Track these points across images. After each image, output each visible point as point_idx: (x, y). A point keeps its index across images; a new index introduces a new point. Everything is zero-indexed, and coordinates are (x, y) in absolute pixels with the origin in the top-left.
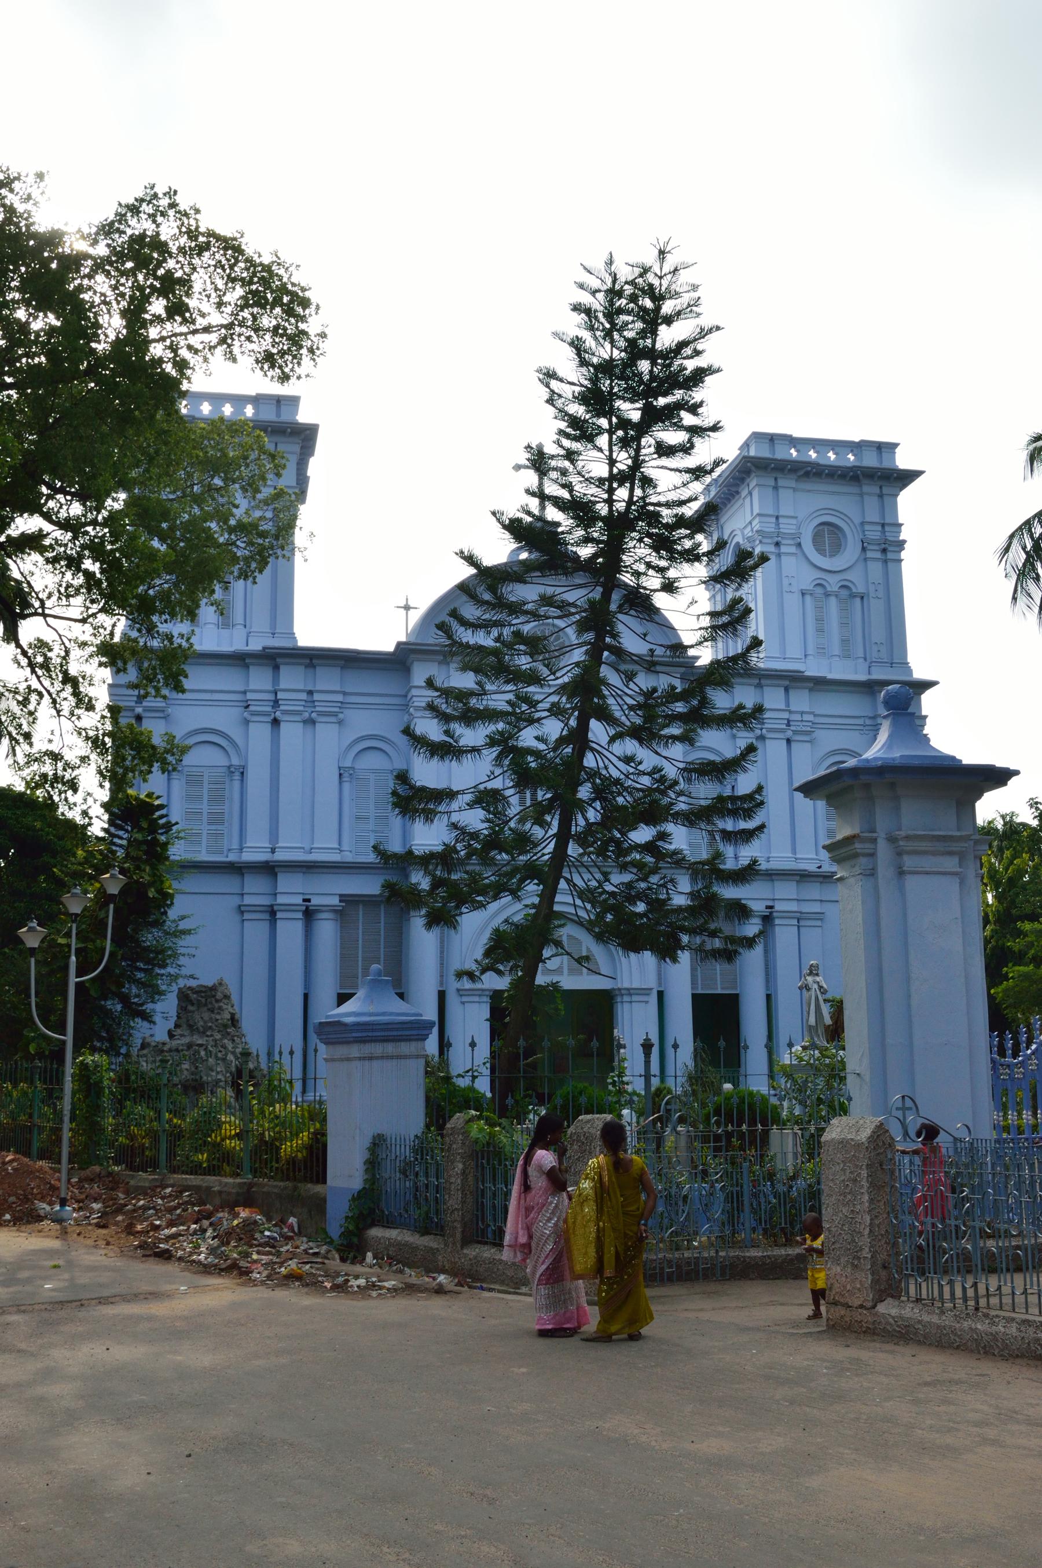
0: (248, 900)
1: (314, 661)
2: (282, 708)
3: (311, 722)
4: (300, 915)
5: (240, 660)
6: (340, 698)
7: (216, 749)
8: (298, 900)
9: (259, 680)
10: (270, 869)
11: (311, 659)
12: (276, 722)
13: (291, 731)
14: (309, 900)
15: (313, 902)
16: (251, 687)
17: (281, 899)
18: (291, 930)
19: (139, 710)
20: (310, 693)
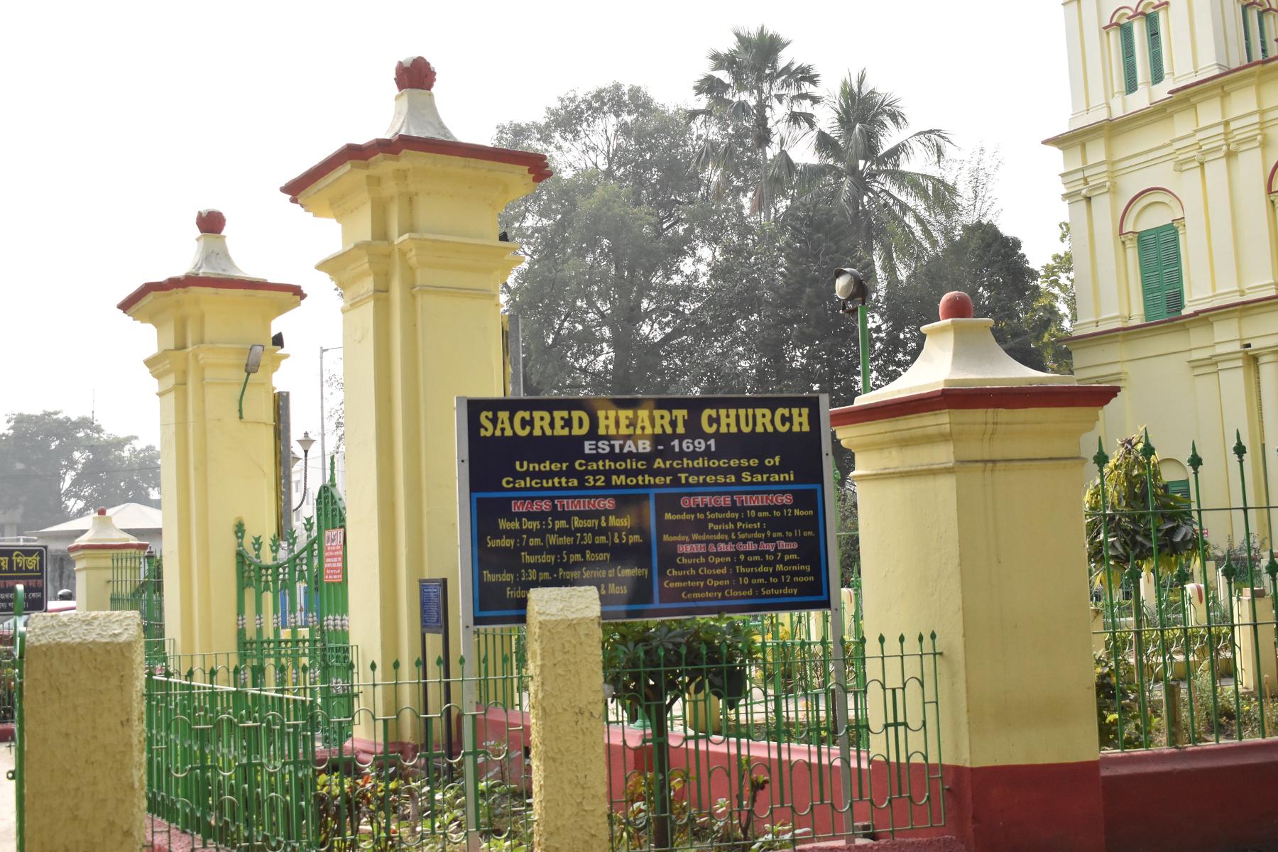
0: (1196, 355)
1: (1225, 89)
2: (1204, 148)
3: (1230, 155)
4: (1240, 363)
5: (1159, 112)
6: (1256, 119)
7: (1158, 207)
8: (1237, 347)
9: (1182, 126)
10: (1205, 317)
11: (1223, 87)
12: (1202, 164)
13: (1217, 169)
14: (1249, 346)
15: (1253, 347)
16: (1178, 136)
17: (1220, 350)
18: (1234, 380)
19: (1084, 192)
20: (1226, 124)
